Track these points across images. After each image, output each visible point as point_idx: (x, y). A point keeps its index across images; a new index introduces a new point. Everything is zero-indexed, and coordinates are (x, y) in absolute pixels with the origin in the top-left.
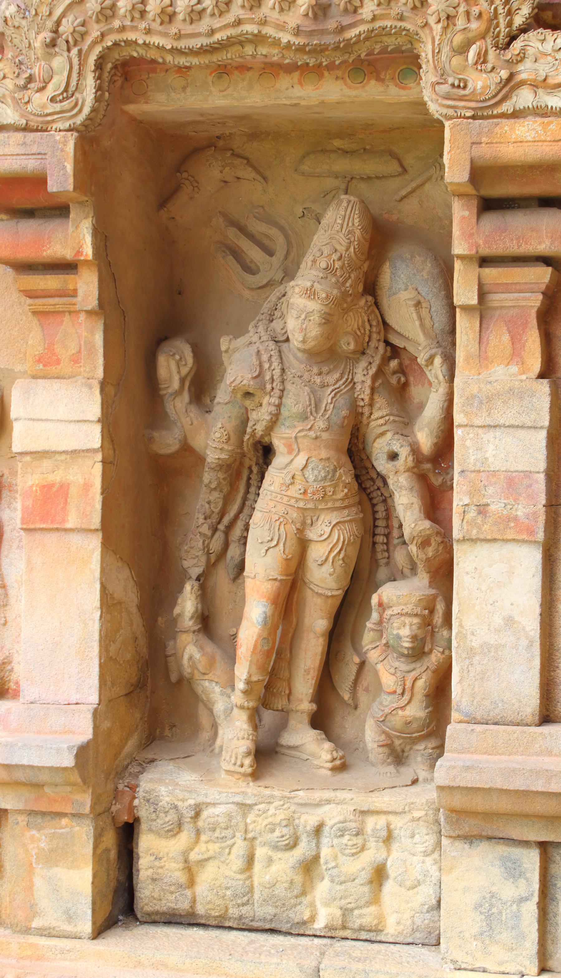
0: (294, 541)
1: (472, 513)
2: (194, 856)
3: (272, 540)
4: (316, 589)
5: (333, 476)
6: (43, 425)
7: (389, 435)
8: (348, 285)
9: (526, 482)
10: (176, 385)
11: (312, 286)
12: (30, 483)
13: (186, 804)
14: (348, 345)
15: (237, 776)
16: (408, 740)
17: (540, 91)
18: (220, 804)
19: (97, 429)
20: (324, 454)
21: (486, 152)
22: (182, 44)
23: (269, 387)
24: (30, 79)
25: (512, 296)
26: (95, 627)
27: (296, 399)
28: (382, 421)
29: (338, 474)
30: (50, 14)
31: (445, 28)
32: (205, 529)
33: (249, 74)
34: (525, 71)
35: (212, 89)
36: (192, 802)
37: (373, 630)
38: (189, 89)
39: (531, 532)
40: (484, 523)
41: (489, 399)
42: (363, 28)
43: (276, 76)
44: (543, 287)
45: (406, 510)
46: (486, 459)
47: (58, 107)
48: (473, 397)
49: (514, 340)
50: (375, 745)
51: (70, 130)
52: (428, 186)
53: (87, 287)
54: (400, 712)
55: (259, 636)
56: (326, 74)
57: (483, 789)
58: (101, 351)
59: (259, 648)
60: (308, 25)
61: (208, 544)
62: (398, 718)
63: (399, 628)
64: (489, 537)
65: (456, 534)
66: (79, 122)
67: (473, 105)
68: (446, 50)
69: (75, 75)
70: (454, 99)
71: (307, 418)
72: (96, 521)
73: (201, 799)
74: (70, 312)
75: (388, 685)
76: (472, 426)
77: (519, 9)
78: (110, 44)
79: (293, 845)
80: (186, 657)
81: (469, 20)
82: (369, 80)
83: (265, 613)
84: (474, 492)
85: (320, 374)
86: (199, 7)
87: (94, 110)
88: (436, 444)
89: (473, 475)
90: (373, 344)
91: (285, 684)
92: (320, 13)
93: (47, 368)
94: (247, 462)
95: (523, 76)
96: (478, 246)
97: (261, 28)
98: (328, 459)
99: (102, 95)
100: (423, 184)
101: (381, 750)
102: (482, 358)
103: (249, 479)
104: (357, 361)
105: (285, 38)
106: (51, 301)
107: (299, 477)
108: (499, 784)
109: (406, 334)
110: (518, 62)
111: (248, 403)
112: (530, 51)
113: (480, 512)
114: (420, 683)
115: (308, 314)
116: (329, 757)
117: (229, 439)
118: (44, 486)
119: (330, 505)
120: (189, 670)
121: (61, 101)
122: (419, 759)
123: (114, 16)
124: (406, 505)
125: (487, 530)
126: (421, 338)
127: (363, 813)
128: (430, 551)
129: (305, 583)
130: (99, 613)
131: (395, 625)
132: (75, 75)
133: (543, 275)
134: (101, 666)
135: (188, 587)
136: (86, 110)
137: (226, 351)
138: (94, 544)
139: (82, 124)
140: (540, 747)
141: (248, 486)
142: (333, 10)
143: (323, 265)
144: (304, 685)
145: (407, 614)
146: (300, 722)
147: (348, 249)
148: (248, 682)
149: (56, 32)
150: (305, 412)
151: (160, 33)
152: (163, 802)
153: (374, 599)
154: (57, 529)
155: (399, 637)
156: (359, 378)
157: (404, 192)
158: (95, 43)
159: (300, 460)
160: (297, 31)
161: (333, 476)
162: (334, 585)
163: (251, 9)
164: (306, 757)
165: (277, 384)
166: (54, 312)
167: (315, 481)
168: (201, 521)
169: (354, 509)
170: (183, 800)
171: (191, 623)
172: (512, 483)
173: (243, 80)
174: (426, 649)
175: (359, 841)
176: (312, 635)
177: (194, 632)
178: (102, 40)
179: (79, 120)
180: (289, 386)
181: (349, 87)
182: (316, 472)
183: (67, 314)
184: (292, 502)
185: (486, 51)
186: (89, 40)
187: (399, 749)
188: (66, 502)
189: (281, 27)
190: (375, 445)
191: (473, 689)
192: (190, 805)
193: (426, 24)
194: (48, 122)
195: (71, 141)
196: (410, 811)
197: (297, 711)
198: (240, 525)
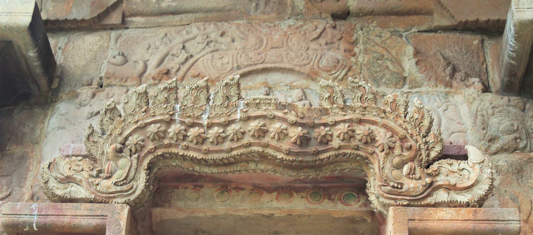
17: (452, 192)
22: (209, 157)
24: (100, 172)
30: (121, 134)
31: (387, 154)
33: (242, 192)
34: (441, 180)
35: (216, 200)
38: (200, 200)
42: (331, 153)
47: (119, 188)
51: (125, 202)
56: (295, 194)
66: (132, 199)
68: (388, 165)
69: (133, 170)
70: (395, 195)
77: (434, 147)
78: (159, 153)
81: (402, 151)
82: (324, 199)
86: (224, 135)
87: (143, 193)
92: (304, 142)
95: (440, 183)
97: (264, 149)
99: (149, 186)
105: (280, 156)
112: (443, 170)
121: (121, 185)
123: (164, 138)
132: (133, 170)
136: (138, 192)
139: (134, 201)
142: (313, 142)
149: (123, 144)
151: (195, 150)
158: (149, 152)
160: (289, 153)
163: (258, 138)
173: (238, 195)
178: (154, 152)
179: (132, 198)
181: (310, 203)
185: (415, 168)
193: (374, 152)
194: (110, 198)
195: (127, 209)
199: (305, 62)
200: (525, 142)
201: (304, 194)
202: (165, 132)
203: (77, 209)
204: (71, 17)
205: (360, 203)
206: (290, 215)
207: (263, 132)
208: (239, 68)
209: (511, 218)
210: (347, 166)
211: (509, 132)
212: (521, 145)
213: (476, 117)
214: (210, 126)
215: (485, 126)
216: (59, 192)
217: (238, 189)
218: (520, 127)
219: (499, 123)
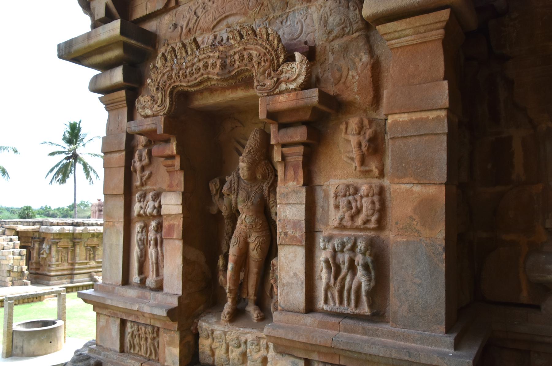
1: (282, 235)
2: (213, 347)
9: (299, 224)
10: (214, 192)
14: (259, 177)
17: (288, 84)
19: (181, 207)
20: (251, 214)
21: (271, 108)
22: (189, 84)
25: (293, 157)
26: (181, 270)
34: (283, 77)
39: (301, 242)
41: (287, 194)
43: (225, 91)
44: (302, 153)
48: (283, 193)
49: (295, 173)
60: (221, 72)
65: (278, 242)
67: (267, 91)
72: (180, 236)
79: (239, 346)
84: (283, 227)
93: (171, 189)
95: (282, 79)
96: (278, 141)
99: (173, 103)
102: (285, 180)
104: (265, 182)
107: (244, 221)
110: (280, 74)
112: (284, 70)
127: (259, 338)
134: (183, 282)
136: (167, 108)
148: (229, 290)
150: (244, 200)
156: (264, 188)
158: (168, 87)
160: (218, 74)
162: (258, 258)
169: (264, 232)
172: (295, 224)
175: (258, 347)
179: (165, 111)
180: (240, 192)
185: (271, 72)
186: (167, 86)
189: (213, 74)
199: (242, 6)
200: (349, 29)
201: (242, 88)
202: (172, 75)
204: (156, 10)
207: (206, 66)
208: (215, 19)
209: (314, 95)
210: (247, 74)
211: (339, 24)
212: (347, 31)
213: (321, 20)
214: (187, 68)
215: (326, 24)
216: (142, 114)
217: (216, 90)
218: (346, 19)
219: (334, 20)
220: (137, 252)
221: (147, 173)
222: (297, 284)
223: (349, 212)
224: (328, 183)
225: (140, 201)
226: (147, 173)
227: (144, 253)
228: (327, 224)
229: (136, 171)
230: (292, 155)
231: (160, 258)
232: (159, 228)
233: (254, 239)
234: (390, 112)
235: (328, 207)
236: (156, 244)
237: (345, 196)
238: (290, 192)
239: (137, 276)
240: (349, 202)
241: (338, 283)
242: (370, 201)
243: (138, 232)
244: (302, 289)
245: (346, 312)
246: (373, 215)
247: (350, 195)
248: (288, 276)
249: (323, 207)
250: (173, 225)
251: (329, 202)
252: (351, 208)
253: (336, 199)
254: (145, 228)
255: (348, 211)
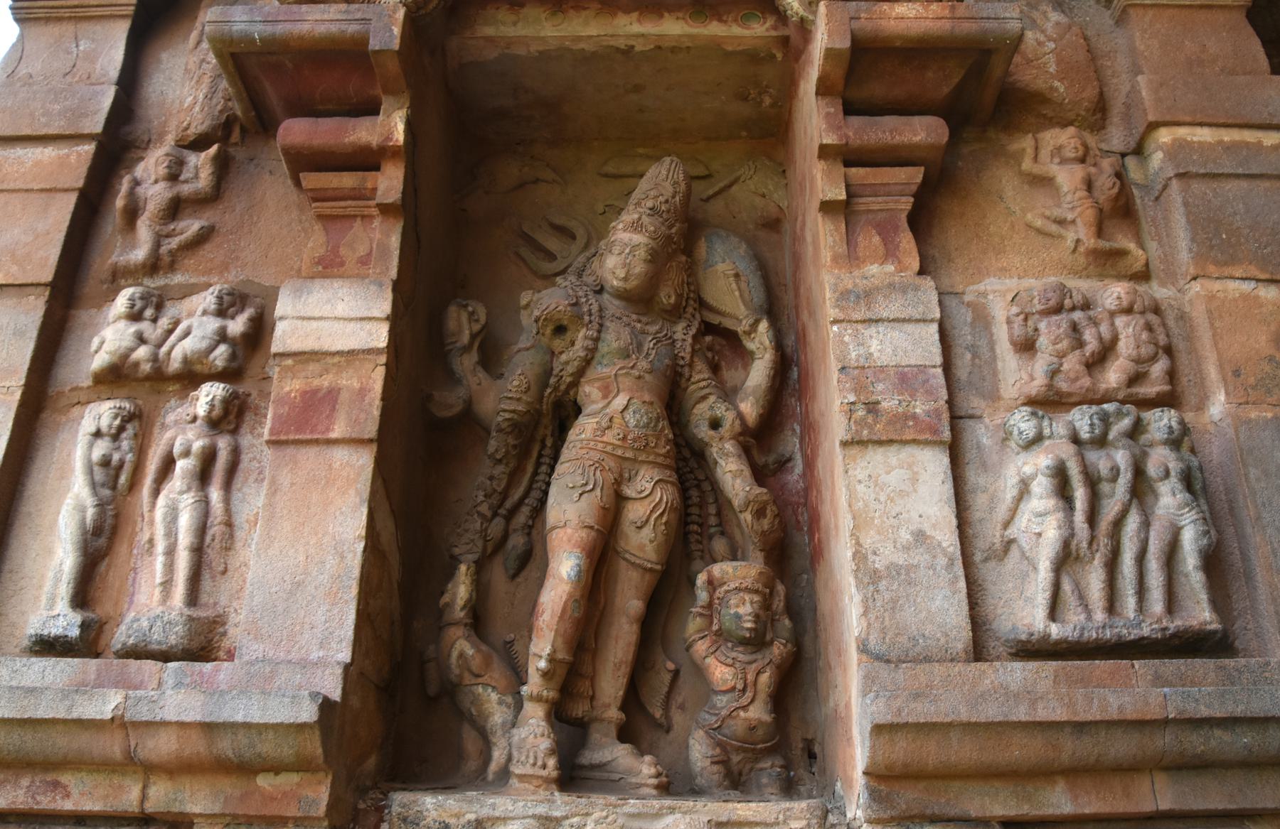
0: (612, 492)
3: (586, 484)
4: (633, 559)
5: (656, 426)
6: (314, 324)
7: (712, 399)
8: (674, 230)
10: (465, 338)
11: (640, 219)
12: (287, 389)
13: (463, 821)
14: (667, 296)
15: (535, 782)
16: (750, 755)
18: (513, 818)
20: (647, 398)
23: (587, 318)
25: (880, 199)
27: (614, 338)
28: (704, 383)
29: (660, 425)
32: (484, 509)
33: (584, 13)
36: (472, 817)
37: (701, 615)
40: (876, 422)
44: (914, 188)
45: (735, 477)
46: (871, 354)
48: (848, 292)
49: (885, 241)
50: (708, 762)
52: (734, 188)
53: (390, 183)
54: (742, 714)
55: (570, 595)
56: (666, 14)
57: (942, 724)
58: (396, 254)
59: (569, 613)
61: (486, 529)
62: (740, 722)
63: (738, 606)
64: (884, 438)
71: (628, 356)
73: (485, 812)
74: (363, 217)
75: (727, 679)
76: (849, 321)
80: (455, 654)
83: (578, 565)
85: (639, 321)
88: (761, 416)
89: (856, 372)
90: (690, 310)
91: (588, 683)
94: (541, 432)
96: (847, 137)
98: (652, 403)
100: (730, 186)
101: (715, 768)
103: (540, 456)
106: (342, 204)
107: (617, 420)
108: (964, 715)
109: (723, 308)
111: (558, 344)
113: (869, 411)
114: (765, 678)
115: (635, 247)
116: (653, 771)
117: (528, 389)
118: (306, 392)
119: (651, 458)
120: (457, 671)
122: (765, 781)
124: (732, 474)
125: (880, 430)
126: (742, 311)
128: (766, 523)
129: (618, 553)
130: (362, 544)
131: (732, 602)
133: (915, 175)
135: (463, 568)
137: (528, 305)
138: (364, 461)
140: (992, 682)
141: (538, 464)
143: (650, 204)
144: (610, 685)
145: (747, 590)
146: (606, 735)
147: (673, 197)
148: (551, 659)
150: (626, 349)
152: (429, 819)
153: (701, 579)
154: (317, 442)
155: (738, 617)
156: (679, 336)
157: (711, 192)
159: (620, 401)
161: (656, 426)
164: (617, 776)
165: (595, 318)
166: (343, 216)
167: (636, 426)
168: (481, 498)
170: (458, 816)
171: (462, 614)
174: (768, 637)
176: (624, 620)
177: (466, 625)
180: (608, 324)
182: (638, 416)
183: (359, 219)
184: (609, 449)
187: (735, 769)
188: (333, 409)
190: (695, 411)
191: (882, 623)
192: (469, 822)
196: (785, 821)
197: (602, 720)
198: (525, 510)
201: (680, 15)
203: (324, 12)
205: (768, 25)
206: (659, 47)
209: (1008, 15)
220: (83, 510)
221: (191, 226)
222: (932, 567)
223: (1077, 352)
224: (981, 287)
225: (134, 316)
226: (191, 226)
227: (109, 521)
228: (993, 396)
229: (132, 213)
230: (875, 190)
231: (215, 530)
232: (229, 418)
233: (649, 486)
234: (1168, 118)
235: (992, 350)
236: (203, 476)
237: (1058, 310)
238: (878, 289)
239: (62, 606)
240: (1075, 327)
241: (1103, 541)
242: (1142, 321)
243: (98, 434)
244: (953, 582)
245: (1134, 634)
246: (1153, 359)
247: (1073, 309)
248: (890, 546)
249: (973, 349)
250: (332, 395)
251: (992, 335)
252: (1080, 344)
253: (1026, 319)
254: (138, 423)
255: (1073, 349)
